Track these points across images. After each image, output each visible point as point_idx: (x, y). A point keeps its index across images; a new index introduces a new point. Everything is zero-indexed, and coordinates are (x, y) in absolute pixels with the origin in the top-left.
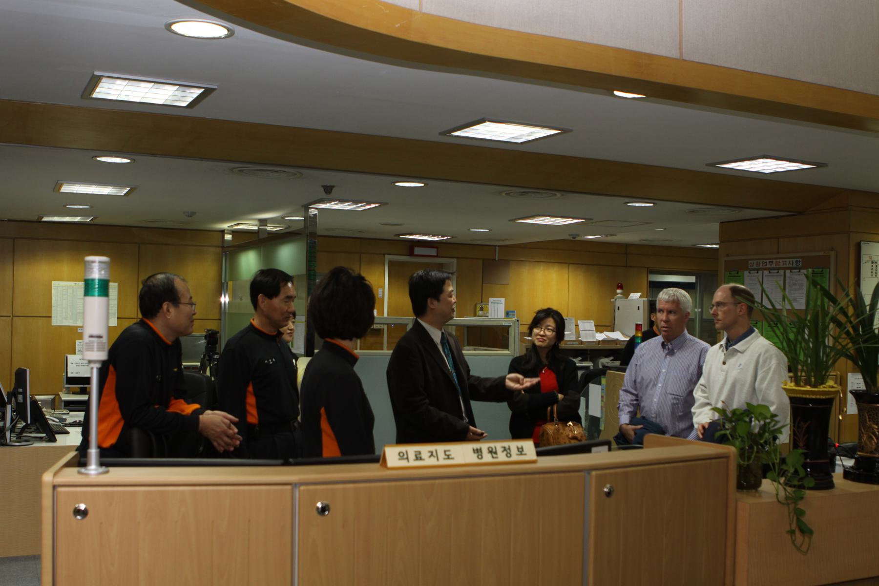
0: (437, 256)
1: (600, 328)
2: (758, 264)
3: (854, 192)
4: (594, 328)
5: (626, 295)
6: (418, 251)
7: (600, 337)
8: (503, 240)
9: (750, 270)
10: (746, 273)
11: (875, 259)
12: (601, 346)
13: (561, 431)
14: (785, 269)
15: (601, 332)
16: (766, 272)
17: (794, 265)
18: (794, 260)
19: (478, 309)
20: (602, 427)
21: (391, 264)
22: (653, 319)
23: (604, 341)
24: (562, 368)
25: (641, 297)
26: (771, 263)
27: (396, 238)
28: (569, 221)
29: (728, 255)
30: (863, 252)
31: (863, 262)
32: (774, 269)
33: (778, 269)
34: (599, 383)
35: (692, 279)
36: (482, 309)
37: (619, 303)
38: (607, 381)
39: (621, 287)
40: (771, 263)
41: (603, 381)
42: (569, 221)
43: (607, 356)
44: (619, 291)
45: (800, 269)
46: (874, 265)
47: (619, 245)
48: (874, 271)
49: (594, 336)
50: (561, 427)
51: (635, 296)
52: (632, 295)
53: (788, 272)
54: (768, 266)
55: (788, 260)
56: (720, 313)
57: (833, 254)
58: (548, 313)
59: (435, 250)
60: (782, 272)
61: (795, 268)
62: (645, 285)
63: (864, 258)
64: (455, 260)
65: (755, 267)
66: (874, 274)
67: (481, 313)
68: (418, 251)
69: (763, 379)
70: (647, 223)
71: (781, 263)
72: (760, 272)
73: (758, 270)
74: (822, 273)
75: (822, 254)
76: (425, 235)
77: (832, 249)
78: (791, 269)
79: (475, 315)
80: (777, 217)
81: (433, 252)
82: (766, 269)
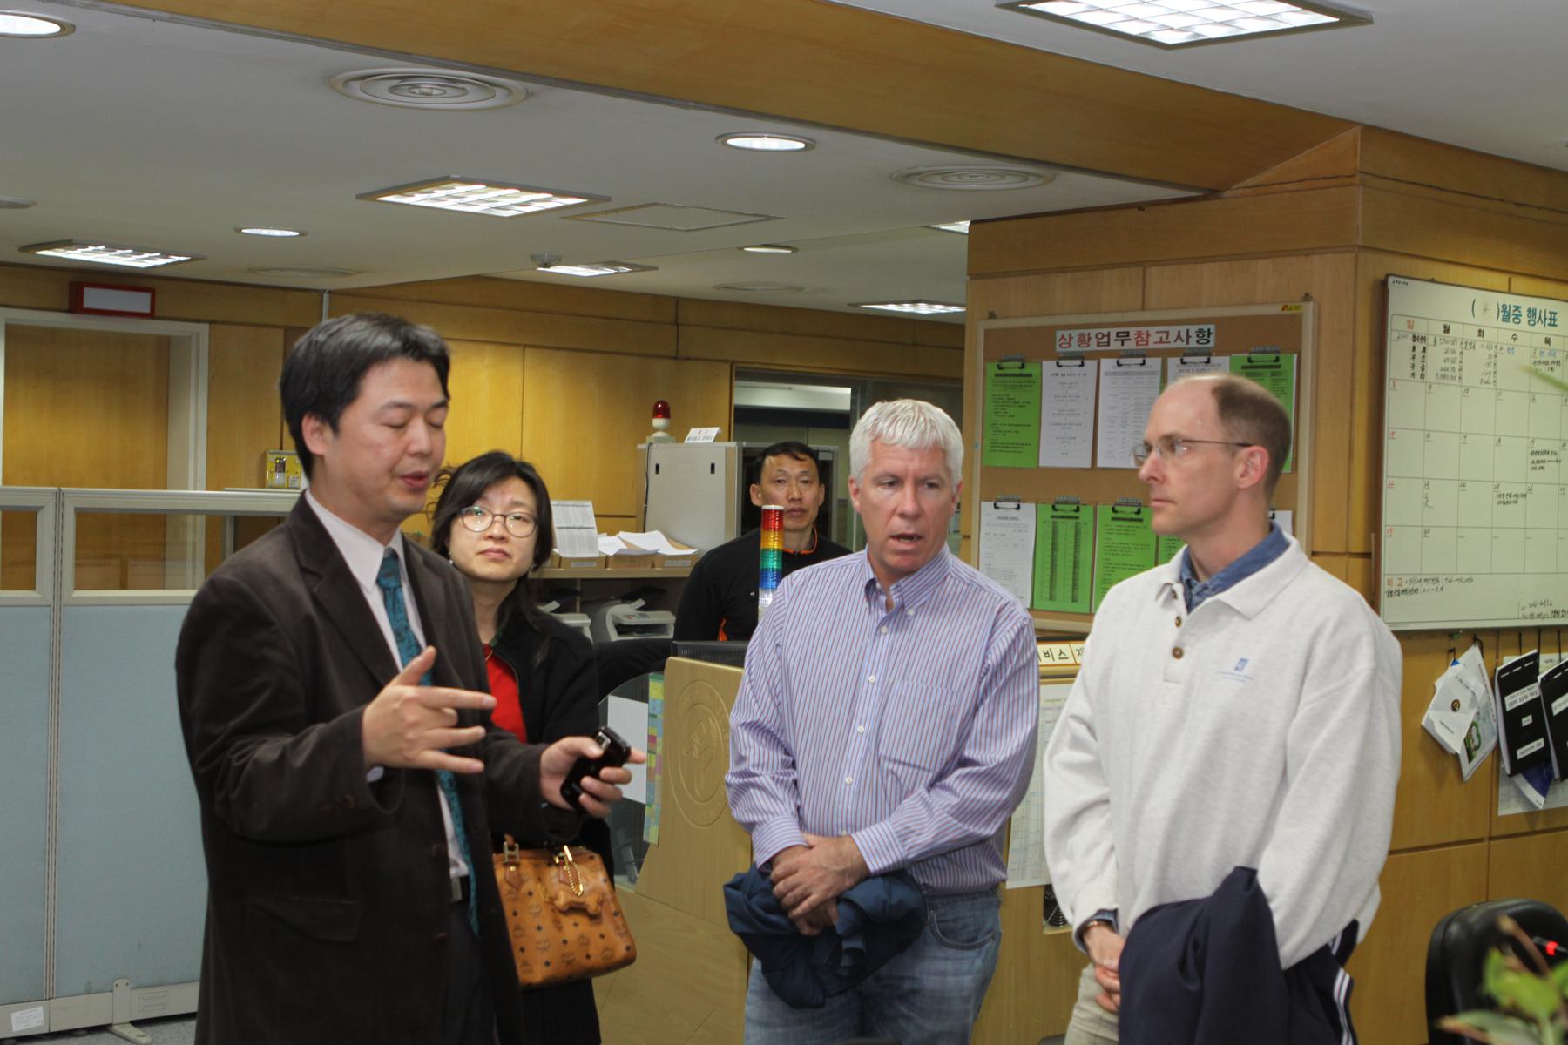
0: (151, 316)
1: (609, 521)
2: (1083, 340)
3: (1370, 131)
4: (593, 522)
5: (678, 433)
6: (94, 298)
7: (610, 545)
8: (344, 274)
9: (1058, 358)
10: (1049, 366)
11: (1419, 329)
12: (611, 572)
13: (530, 885)
14: (1165, 354)
15: (612, 533)
16: (1108, 364)
17: (1193, 344)
18: (1194, 329)
19: (271, 466)
20: (651, 834)
21: (15, 335)
22: (756, 501)
23: (619, 558)
24: (539, 658)
25: (718, 438)
26: (1123, 338)
27: (25, 258)
28: (542, 202)
29: (992, 316)
30: (1393, 308)
31: (1391, 335)
32: (1131, 354)
33: (1144, 355)
34: (643, 696)
35: (839, 397)
36: (281, 467)
37: (657, 456)
38: (668, 694)
39: (663, 411)
40: (1123, 338)
41: (656, 687)
42: (542, 202)
43: (628, 598)
44: (658, 422)
45: (1208, 353)
46: (1419, 346)
47: (656, 300)
48: (1418, 365)
49: (593, 544)
50: (527, 867)
51: (703, 436)
52: (693, 432)
53: (1173, 362)
54: (1115, 345)
55: (1174, 330)
56: (1172, 474)
57: (1308, 309)
58: (499, 467)
59: (147, 297)
60: (1154, 363)
61: (1195, 353)
62: (725, 414)
63: (1395, 324)
64: (204, 329)
65: (1075, 347)
66: (1418, 371)
67: (278, 478)
68: (94, 298)
69: (1318, 719)
70: (769, 218)
71: (1154, 338)
72: (1090, 365)
73: (1082, 357)
74: (1275, 365)
75: (1276, 310)
76: (111, 247)
77: (1307, 298)
78: (1183, 354)
79: (262, 484)
80: (1140, 206)
81: (141, 302)
82: (1109, 354)
